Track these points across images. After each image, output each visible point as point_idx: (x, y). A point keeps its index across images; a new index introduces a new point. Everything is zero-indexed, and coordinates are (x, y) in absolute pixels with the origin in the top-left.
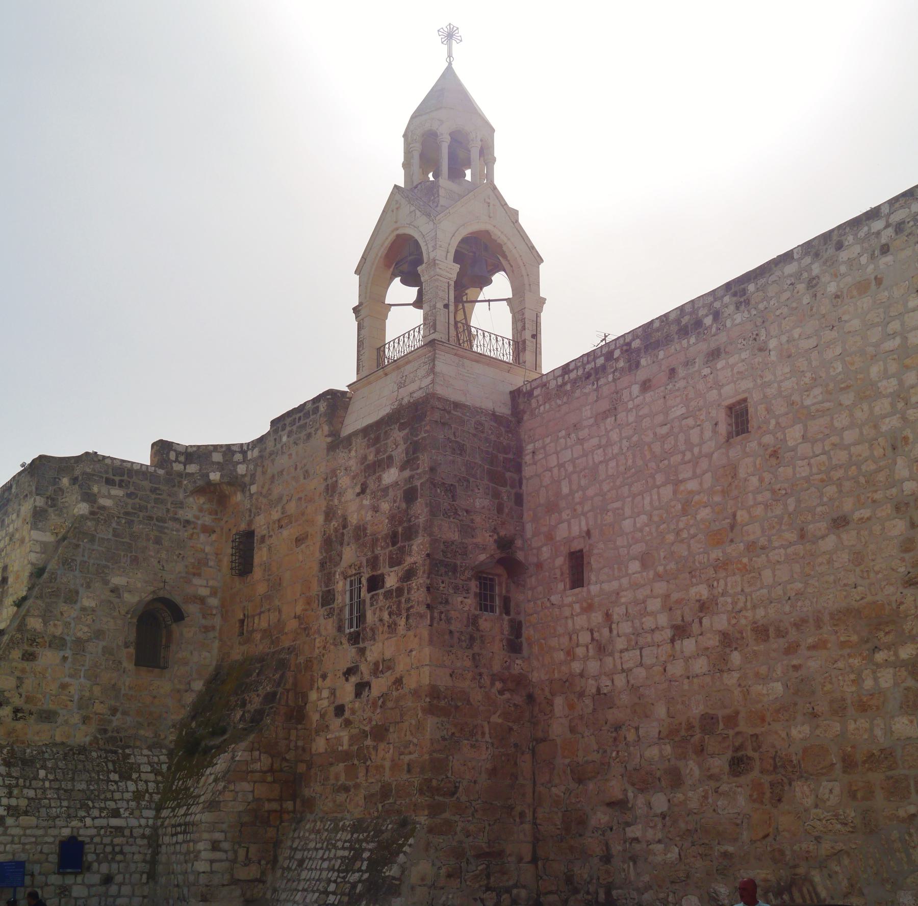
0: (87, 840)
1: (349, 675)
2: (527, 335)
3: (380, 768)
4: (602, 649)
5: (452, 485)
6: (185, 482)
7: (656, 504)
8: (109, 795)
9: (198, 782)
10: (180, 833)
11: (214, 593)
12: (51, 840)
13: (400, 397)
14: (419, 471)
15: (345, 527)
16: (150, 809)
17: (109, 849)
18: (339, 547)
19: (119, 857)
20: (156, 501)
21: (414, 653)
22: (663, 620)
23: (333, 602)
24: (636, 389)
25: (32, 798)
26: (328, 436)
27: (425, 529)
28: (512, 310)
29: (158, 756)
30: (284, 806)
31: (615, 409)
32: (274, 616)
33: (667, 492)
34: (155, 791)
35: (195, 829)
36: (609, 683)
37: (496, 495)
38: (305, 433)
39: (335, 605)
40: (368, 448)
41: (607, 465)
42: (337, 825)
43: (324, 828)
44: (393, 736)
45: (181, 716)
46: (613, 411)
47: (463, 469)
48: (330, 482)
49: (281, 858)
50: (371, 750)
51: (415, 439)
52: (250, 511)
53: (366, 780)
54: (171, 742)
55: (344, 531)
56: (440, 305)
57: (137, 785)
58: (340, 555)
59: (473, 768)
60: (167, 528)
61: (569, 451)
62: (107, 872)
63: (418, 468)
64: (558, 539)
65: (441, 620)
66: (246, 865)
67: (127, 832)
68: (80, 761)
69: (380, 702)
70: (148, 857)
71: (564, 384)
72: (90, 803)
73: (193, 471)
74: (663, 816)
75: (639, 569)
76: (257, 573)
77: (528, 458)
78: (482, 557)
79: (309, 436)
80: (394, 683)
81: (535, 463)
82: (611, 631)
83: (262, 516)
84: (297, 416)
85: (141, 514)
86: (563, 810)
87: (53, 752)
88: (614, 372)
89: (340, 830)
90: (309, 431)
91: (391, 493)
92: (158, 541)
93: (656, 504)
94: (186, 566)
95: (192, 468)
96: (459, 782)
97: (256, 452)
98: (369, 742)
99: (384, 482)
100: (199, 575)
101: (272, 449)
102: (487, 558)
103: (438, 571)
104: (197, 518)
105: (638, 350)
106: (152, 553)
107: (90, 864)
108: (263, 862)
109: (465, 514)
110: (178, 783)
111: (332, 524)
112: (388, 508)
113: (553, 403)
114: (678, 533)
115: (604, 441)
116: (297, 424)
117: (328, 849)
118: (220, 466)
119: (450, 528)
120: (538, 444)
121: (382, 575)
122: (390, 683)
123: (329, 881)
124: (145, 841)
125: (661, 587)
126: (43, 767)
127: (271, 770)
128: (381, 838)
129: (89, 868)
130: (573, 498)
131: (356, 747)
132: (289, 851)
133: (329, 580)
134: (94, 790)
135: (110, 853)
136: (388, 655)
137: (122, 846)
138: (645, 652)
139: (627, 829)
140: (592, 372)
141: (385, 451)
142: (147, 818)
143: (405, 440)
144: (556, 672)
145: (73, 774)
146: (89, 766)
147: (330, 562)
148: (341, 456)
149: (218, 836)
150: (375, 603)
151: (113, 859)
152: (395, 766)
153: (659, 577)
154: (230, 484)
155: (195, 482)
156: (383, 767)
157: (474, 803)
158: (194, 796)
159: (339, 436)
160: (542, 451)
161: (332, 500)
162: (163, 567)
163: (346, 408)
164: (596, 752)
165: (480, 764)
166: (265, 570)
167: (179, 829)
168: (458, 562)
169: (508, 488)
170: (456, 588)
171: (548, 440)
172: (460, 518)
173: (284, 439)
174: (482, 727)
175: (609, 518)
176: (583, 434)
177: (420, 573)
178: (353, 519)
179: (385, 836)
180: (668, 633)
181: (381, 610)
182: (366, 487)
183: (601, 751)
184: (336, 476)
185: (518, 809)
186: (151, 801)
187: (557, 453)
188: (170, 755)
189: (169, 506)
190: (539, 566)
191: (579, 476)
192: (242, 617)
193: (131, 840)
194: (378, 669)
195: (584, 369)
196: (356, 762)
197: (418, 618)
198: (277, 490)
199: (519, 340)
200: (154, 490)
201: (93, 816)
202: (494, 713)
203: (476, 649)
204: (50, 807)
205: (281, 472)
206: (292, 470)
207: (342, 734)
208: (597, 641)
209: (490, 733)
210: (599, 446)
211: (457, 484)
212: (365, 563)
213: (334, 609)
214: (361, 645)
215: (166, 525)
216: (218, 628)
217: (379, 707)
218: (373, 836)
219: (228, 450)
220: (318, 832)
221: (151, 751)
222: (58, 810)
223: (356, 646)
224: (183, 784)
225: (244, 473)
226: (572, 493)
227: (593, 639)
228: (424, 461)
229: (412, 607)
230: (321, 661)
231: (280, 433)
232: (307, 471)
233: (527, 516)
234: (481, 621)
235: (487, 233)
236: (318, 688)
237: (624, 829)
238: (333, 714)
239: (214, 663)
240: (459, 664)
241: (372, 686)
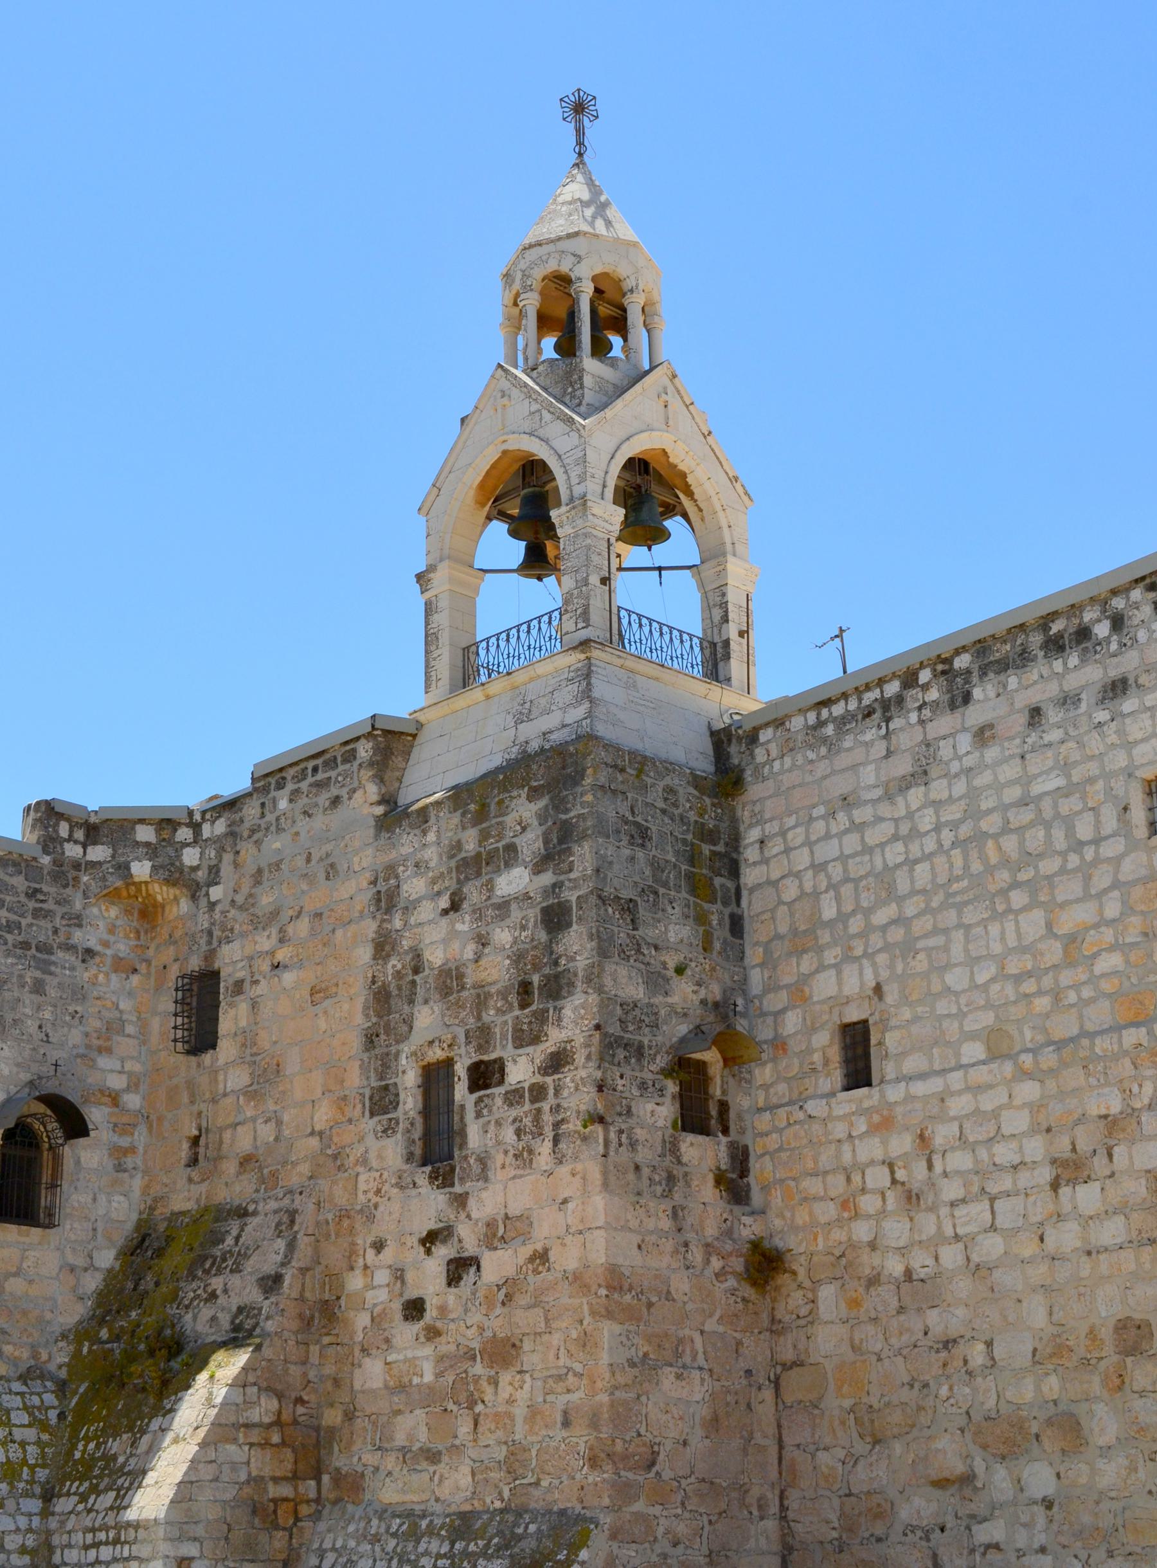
1: (432, 1243)
2: (732, 631)
3: (504, 1419)
4: (912, 1198)
5: (631, 900)
6: (85, 879)
7: (1012, 942)
9: (134, 1444)
10: (107, 1543)
11: (133, 1085)
13: (522, 739)
14: (572, 876)
15: (416, 971)
16: (33, 1496)
18: (406, 1007)
20: (37, 913)
21: (571, 1206)
22: (1035, 1148)
23: (396, 1108)
24: (965, 742)
26: (379, 803)
27: (588, 980)
28: (701, 585)
29: (39, 1394)
30: (301, 1490)
31: (925, 773)
32: (266, 1132)
33: (1033, 923)
34: (40, 1461)
35: (141, 1534)
36: (930, 1262)
37: (701, 919)
38: (328, 795)
39: (399, 1113)
40: (464, 828)
41: (912, 870)
42: (415, 1526)
43: (387, 1531)
44: (531, 1358)
45: (77, 1318)
46: (921, 776)
47: (648, 872)
48: (382, 886)
50: (484, 1383)
51: (563, 817)
52: (210, 933)
53: (475, 1441)
54: (60, 1367)
56: (594, 580)
57: (7, 1451)
58: (409, 1023)
59: (681, 1418)
60: (54, 963)
61: (835, 841)
63: (571, 870)
64: (815, 999)
65: (620, 1145)
69: (501, 1296)
71: (821, 724)
73: (101, 859)
74: (1048, 1504)
75: (983, 1057)
76: (226, 1049)
77: (751, 854)
78: (683, 1029)
79: (336, 801)
80: (531, 1259)
81: (765, 861)
82: (930, 1166)
83: (236, 945)
84: (310, 765)
85: (9, 937)
86: (841, 1493)
88: (920, 708)
90: (334, 791)
91: (516, 914)
92: (38, 988)
93: (1012, 942)
94: (87, 1035)
95: (98, 853)
96: (659, 1444)
97: (220, 827)
98: (478, 1369)
99: (499, 893)
100: (109, 1051)
101: (259, 822)
102: (690, 1032)
103: (613, 1056)
104: (106, 944)
105: (968, 672)
106: (28, 1011)
109: (653, 952)
110: (86, 1446)
111: (390, 966)
112: (510, 939)
113: (799, 757)
114: (1057, 995)
115: (904, 829)
116: (310, 779)
118: (152, 851)
119: (630, 978)
120: (772, 828)
122: (521, 1261)
125: (1029, 1091)
127: (278, 1423)
128: (516, 1550)
130: (846, 927)
131: (450, 1378)
133: (386, 1066)
136: (514, 1210)
138: (998, 1204)
139: (974, 1528)
140: (876, 705)
141: (500, 837)
142: (30, 1515)
143: (542, 818)
144: (820, 1240)
147: (387, 1034)
148: (407, 843)
149: (191, 1550)
150: (485, 1112)
152: (533, 1412)
153: (1025, 1074)
154: (170, 882)
155: (104, 879)
156: (509, 1415)
157: (684, 1482)
158: (129, 1473)
159: (396, 803)
160: (779, 840)
161: (390, 921)
162: (47, 1036)
163: (407, 754)
164: (907, 1387)
165: (691, 1410)
166: (244, 1045)
167: (102, 1536)
168: (646, 1043)
169: (719, 905)
170: (643, 1086)
171: (791, 821)
172: (647, 959)
173: (283, 804)
174: (692, 1341)
175: (920, 963)
176: (862, 814)
177: (580, 1058)
178: (435, 957)
180: (1046, 1174)
181: (498, 1123)
182: (462, 900)
183: (917, 1385)
184: (397, 877)
185: (755, 1492)
186: (32, 1482)
187: (809, 844)
188: (62, 1388)
189: (58, 921)
190: (779, 1045)
191: (856, 889)
192: (195, 1132)
194: (494, 1235)
195: (860, 700)
196: (451, 1406)
197: (578, 1142)
198: (266, 900)
199: (717, 639)
200: (32, 894)
202: (711, 1316)
203: (678, 1196)
205: (277, 865)
206: (300, 861)
207: (419, 1353)
208: (903, 1184)
209: (705, 1353)
210: (895, 838)
211: (639, 900)
212: (462, 1038)
213: (397, 1123)
214: (458, 1189)
215: (53, 958)
216: (141, 1150)
217: (499, 1305)
219: (166, 823)
220: (376, 1539)
221: (27, 1385)
223: (447, 1190)
224: (98, 1446)
225: (195, 863)
226: (843, 918)
227: (894, 1181)
228: (583, 856)
229: (563, 1120)
230: (371, 1219)
231: (273, 794)
232: (332, 865)
233: (754, 955)
234: (683, 1147)
236: (366, 1267)
237: (968, 1528)
238: (398, 1316)
239: (134, 1217)
240: (651, 1226)
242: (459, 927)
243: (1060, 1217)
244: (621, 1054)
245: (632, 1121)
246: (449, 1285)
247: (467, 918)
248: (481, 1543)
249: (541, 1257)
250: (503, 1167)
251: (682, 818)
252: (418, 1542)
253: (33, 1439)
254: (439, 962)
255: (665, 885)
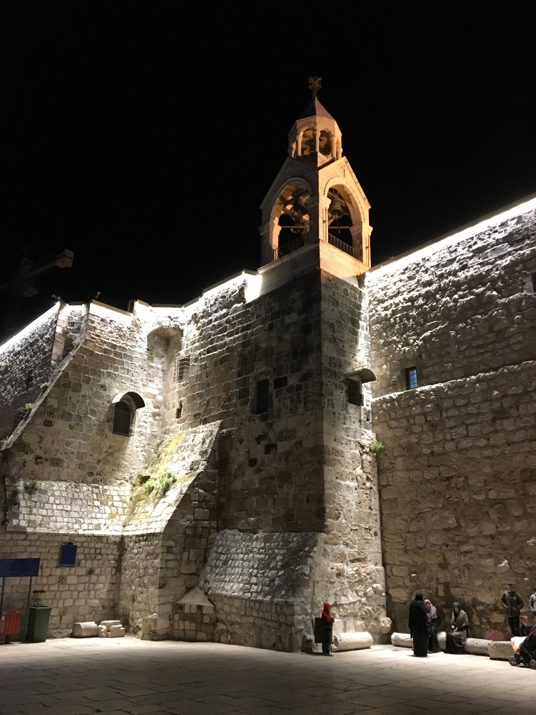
0: (79, 545)
8: (94, 515)
12: (56, 544)
14: (313, 314)
15: (256, 350)
17: (93, 551)
19: (99, 557)
21: (311, 425)
22: (485, 407)
25: (45, 516)
47: (338, 315)
49: (209, 559)
55: (257, 353)
62: (90, 566)
66: (187, 564)
67: (104, 540)
68: (76, 492)
70: (116, 557)
72: (82, 520)
80: (296, 444)
87: (59, 485)
89: (254, 540)
91: (292, 328)
98: (275, 482)
107: (80, 561)
108: (198, 562)
117: (247, 553)
121: (286, 378)
123: (251, 575)
124: (116, 546)
126: (53, 495)
129: (79, 565)
132: (215, 554)
134: (85, 511)
135: (93, 554)
137: (101, 549)
145: (72, 500)
146: (82, 496)
149: (171, 543)
150: (280, 395)
151: (95, 558)
170: (336, 386)
179: (292, 545)
180: (490, 417)
193: (108, 545)
201: (84, 528)
204: (56, 522)
208: (430, 421)
214: (269, 421)
218: (282, 546)
222: (62, 524)
227: (427, 421)
235: (342, 186)
236: (236, 449)
241: (278, 447)
242: (272, 335)
243: (496, 432)
244: (329, 374)
245: (332, 398)
246: (266, 454)
247: (275, 332)
248: (276, 544)
249: (299, 443)
250: (286, 413)
251: (349, 300)
252: (252, 543)
253: (121, 506)
254: (264, 347)
255: (344, 321)
